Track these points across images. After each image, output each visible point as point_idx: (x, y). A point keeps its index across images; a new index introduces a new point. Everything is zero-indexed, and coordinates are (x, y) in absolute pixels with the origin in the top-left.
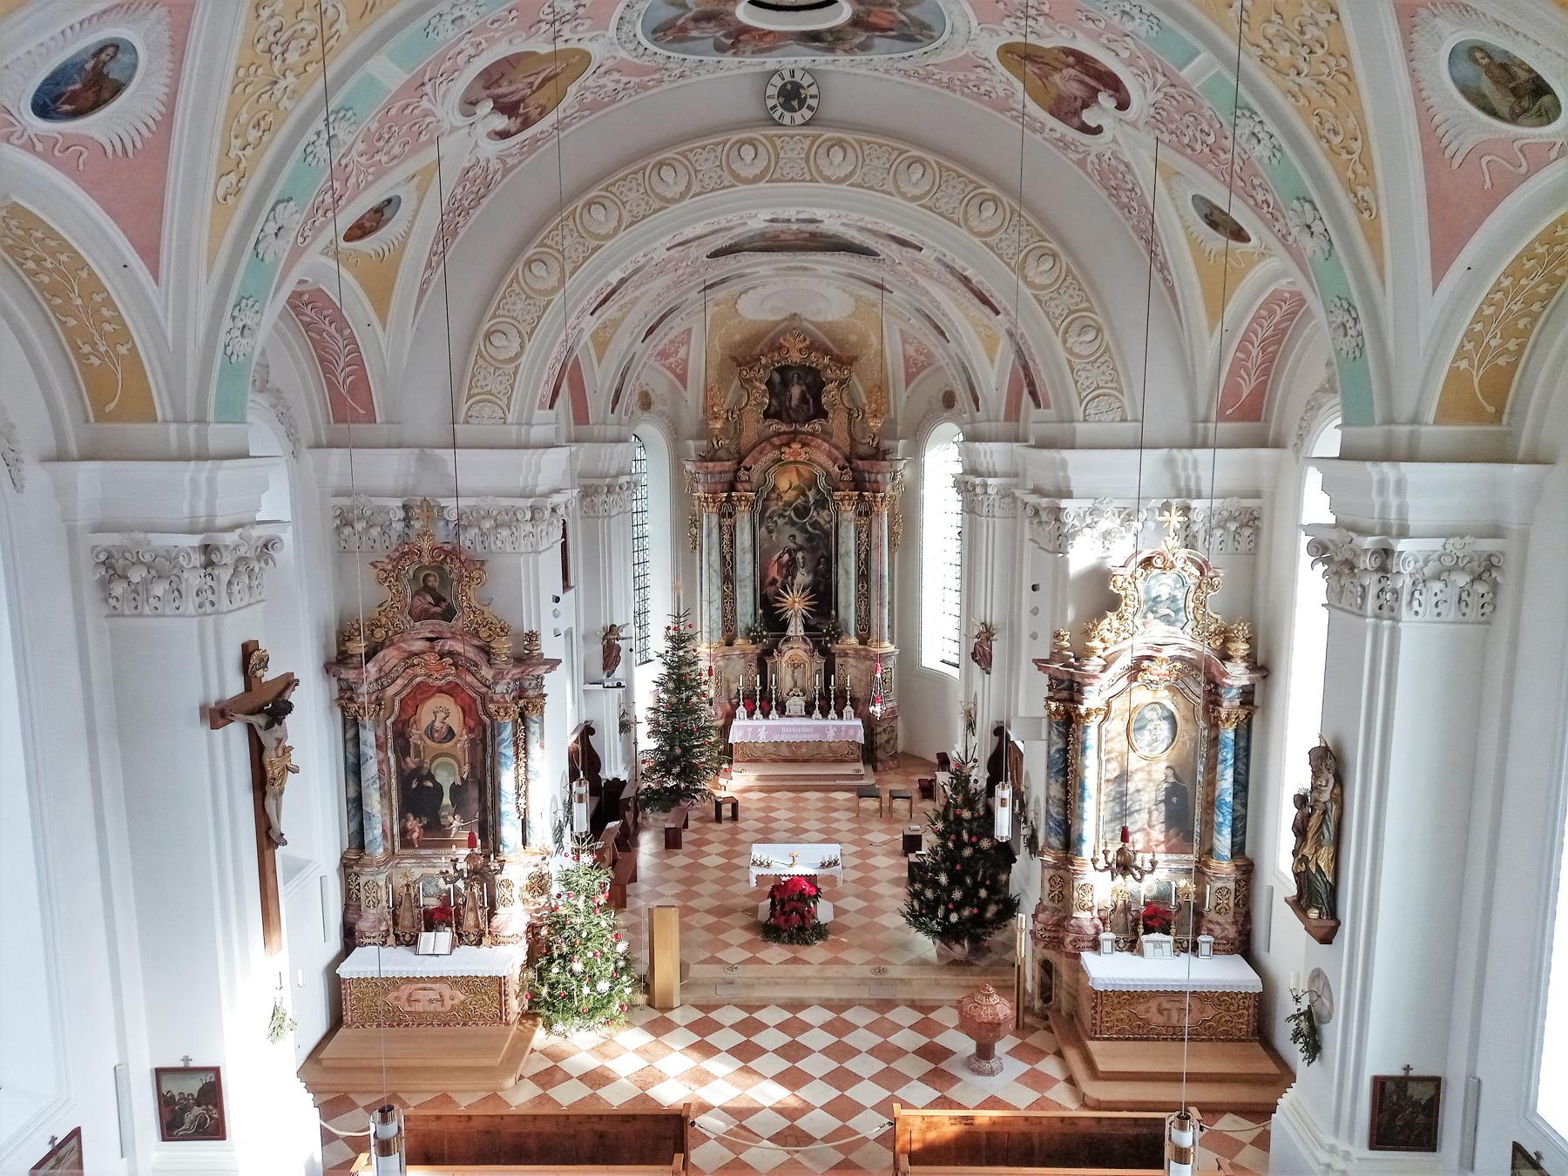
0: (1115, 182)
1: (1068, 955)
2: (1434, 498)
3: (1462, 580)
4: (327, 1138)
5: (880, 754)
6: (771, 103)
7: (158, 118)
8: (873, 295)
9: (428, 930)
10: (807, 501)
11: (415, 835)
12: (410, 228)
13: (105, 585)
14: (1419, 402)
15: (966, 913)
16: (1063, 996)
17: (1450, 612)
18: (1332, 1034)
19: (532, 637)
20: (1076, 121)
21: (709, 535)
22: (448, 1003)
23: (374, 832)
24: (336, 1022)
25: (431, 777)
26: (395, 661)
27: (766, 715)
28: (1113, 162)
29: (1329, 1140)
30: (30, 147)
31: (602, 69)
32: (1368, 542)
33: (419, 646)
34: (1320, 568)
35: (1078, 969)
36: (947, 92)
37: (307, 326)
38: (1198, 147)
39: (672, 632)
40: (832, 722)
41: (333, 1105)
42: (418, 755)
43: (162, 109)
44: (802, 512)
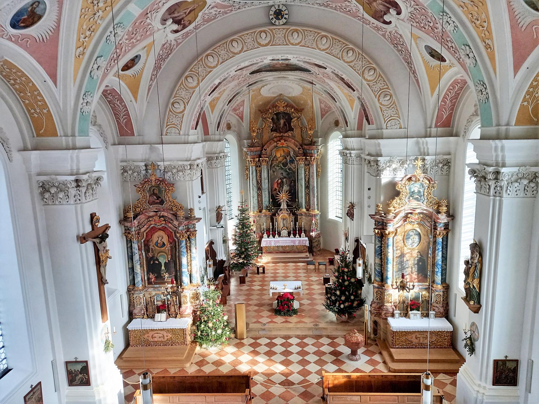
0: (397, 42)
1: (383, 319)
2: (514, 152)
3: (525, 182)
4: (126, 385)
5: (314, 250)
6: (271, 17)
7: (54, 27)
8: (309, 86)
9: (159, 312)
10: (287, 161)
11: (153, 280)
12: (144, 66)
13: (42, 194)
14: (509, 118)
15: (347, 304)
16: (381, 333)
17: (521, 194)
18: (479, 345)
19: (191, 210)
20: (382, 20)
21: (252, 174)
22: (166, 338)
23: (138, 279)
24: (127, 345)
25: (157, 260)
26: (144, 219)
27: (274, 237)
28: (395, 34)
29: (478, 382)
30: (10, 39)
31: (211, 7)
32: (491, 169)
33: (152, 214)
34: (473, 179)
35: (387, 324)
36: (334, 11)
37: (109, 102)
38: (427, 27)
39: (240, 208)
40: (297, 238)
41: (127, 374)
42: (153, 252)
43: (56, 24)
44: (285, 165)
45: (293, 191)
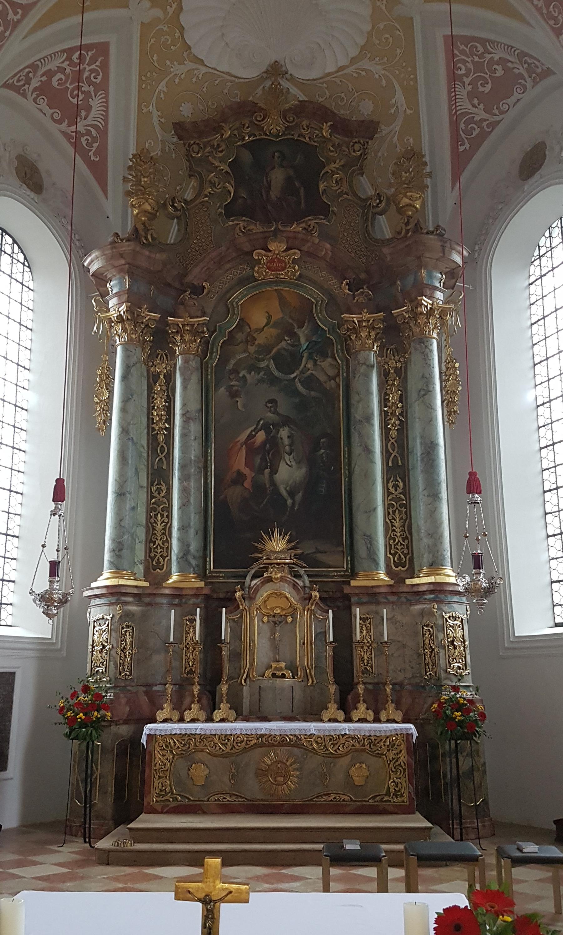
44: (288, 361)
45: (323, 488)
